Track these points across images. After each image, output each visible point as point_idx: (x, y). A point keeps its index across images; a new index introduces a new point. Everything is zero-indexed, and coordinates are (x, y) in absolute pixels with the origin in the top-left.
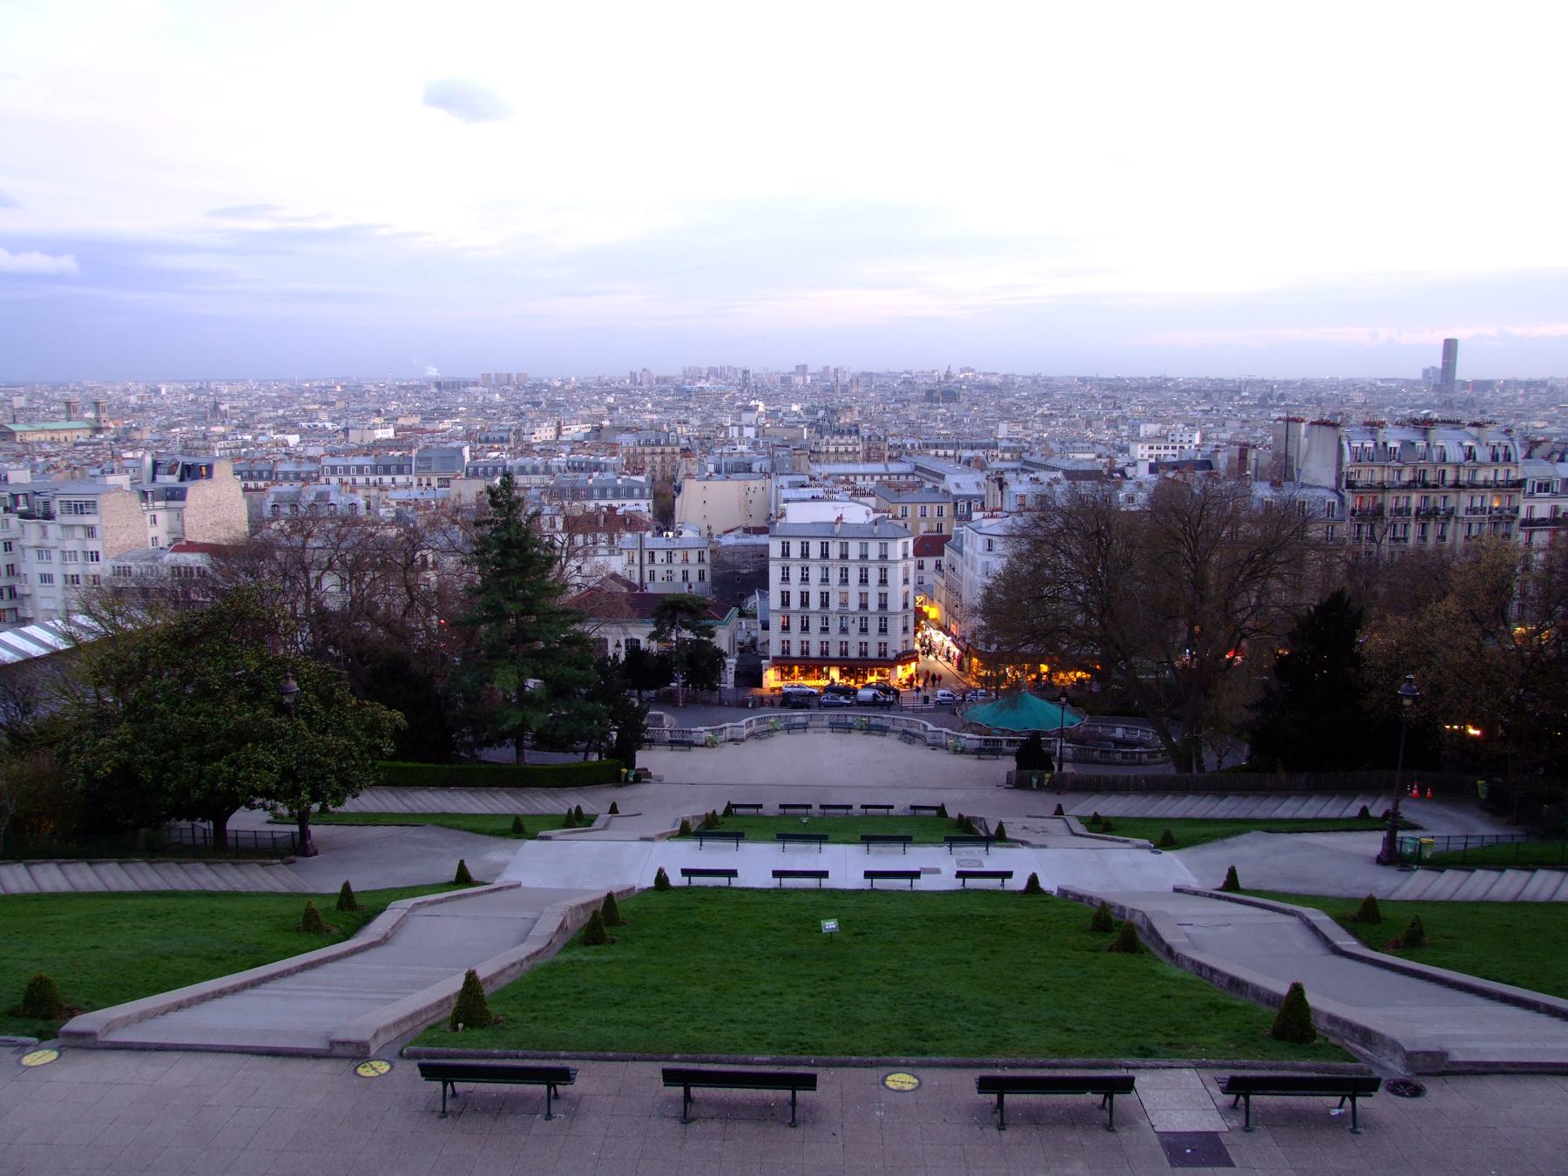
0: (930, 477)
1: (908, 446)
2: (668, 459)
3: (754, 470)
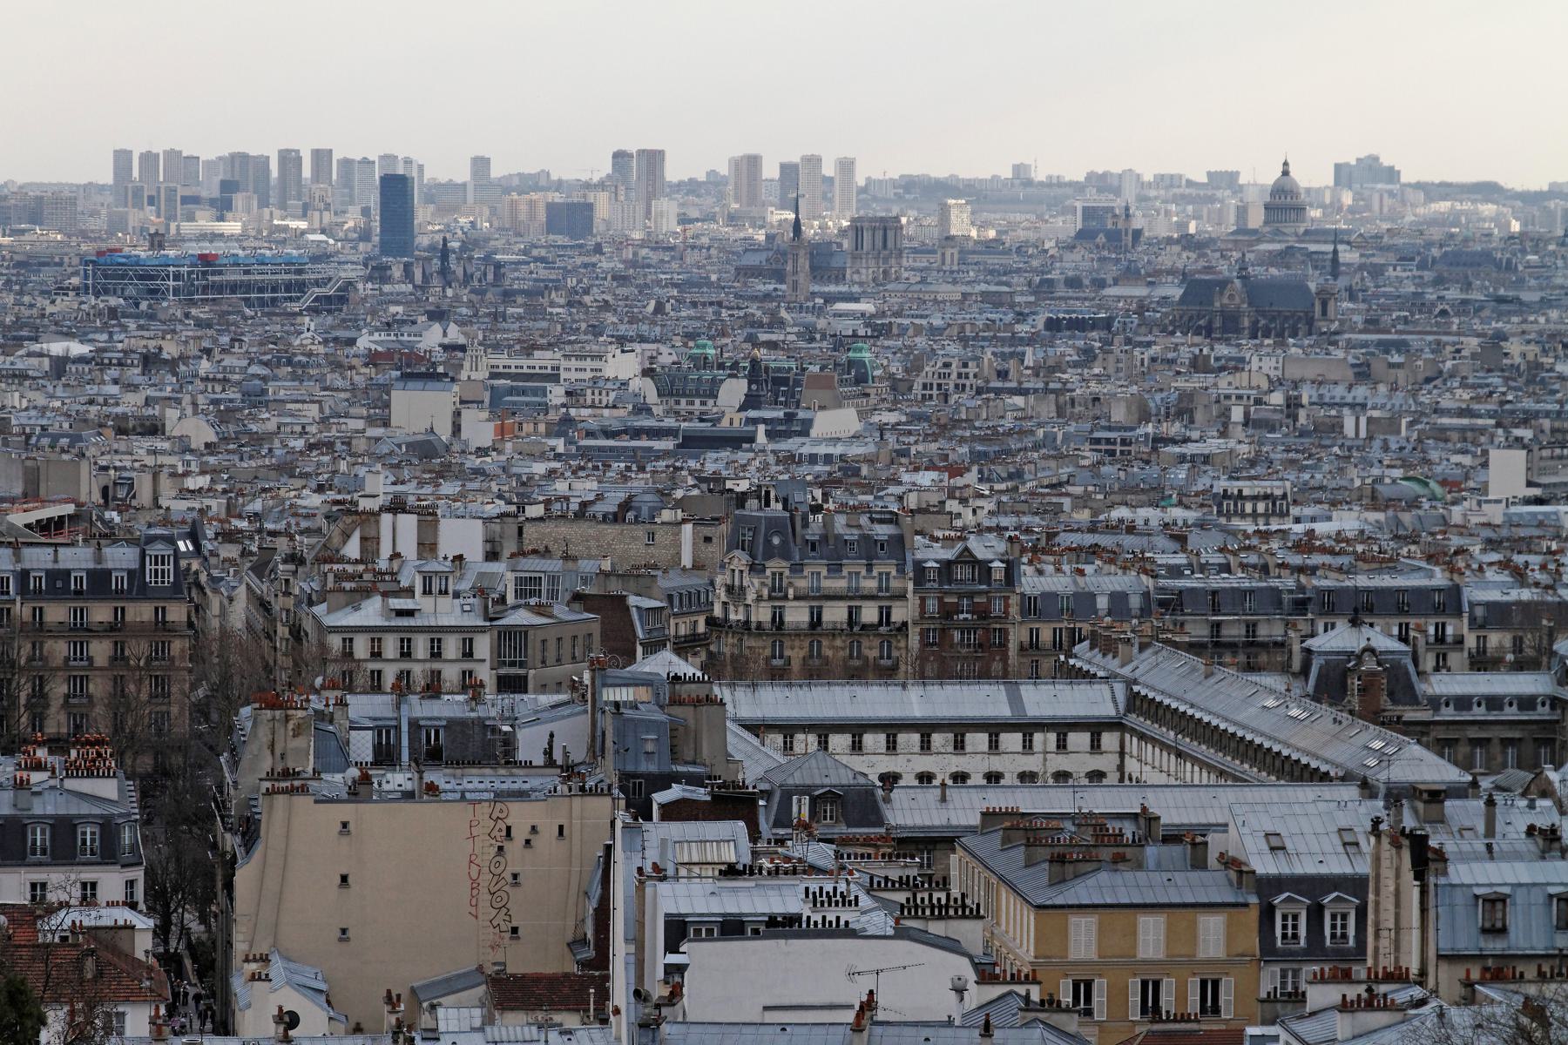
0: (1186, 743)
1: (1102, 603)
2: (138, 649)
3: (521, 756)
